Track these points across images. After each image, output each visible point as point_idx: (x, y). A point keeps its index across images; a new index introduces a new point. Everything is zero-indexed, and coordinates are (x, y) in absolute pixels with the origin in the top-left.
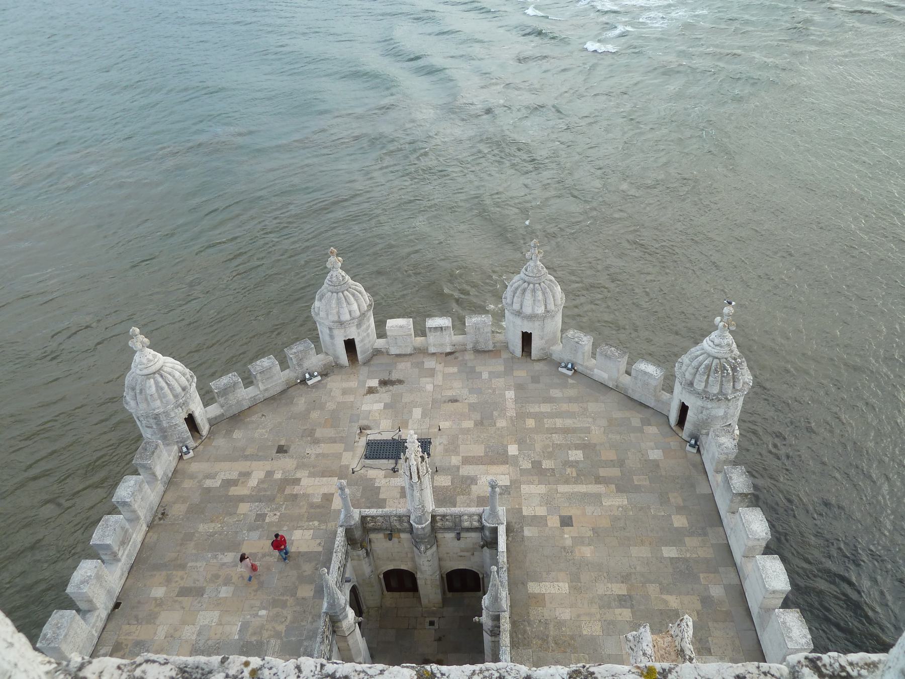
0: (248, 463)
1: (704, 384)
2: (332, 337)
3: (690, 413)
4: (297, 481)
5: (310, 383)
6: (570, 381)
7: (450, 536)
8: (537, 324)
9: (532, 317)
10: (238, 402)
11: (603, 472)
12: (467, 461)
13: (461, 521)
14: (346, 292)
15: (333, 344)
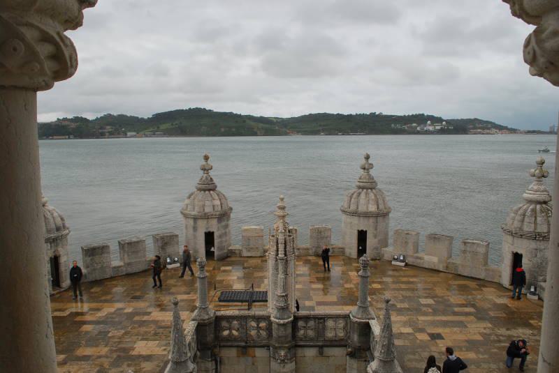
0: (101, 304)
1: (533, 225)
2: (195, 229)
3: (524, 261)
4: (149, 313)
5: (169, 267)
6: (404, 268)
7: (310, 353)
8: (371, 220)
9: (366, 215)
10: (102, 267)
11: (456, 309)
12: (319, 304)
13: (324, 328)
14: (211, 192)
15: (195, 237)
